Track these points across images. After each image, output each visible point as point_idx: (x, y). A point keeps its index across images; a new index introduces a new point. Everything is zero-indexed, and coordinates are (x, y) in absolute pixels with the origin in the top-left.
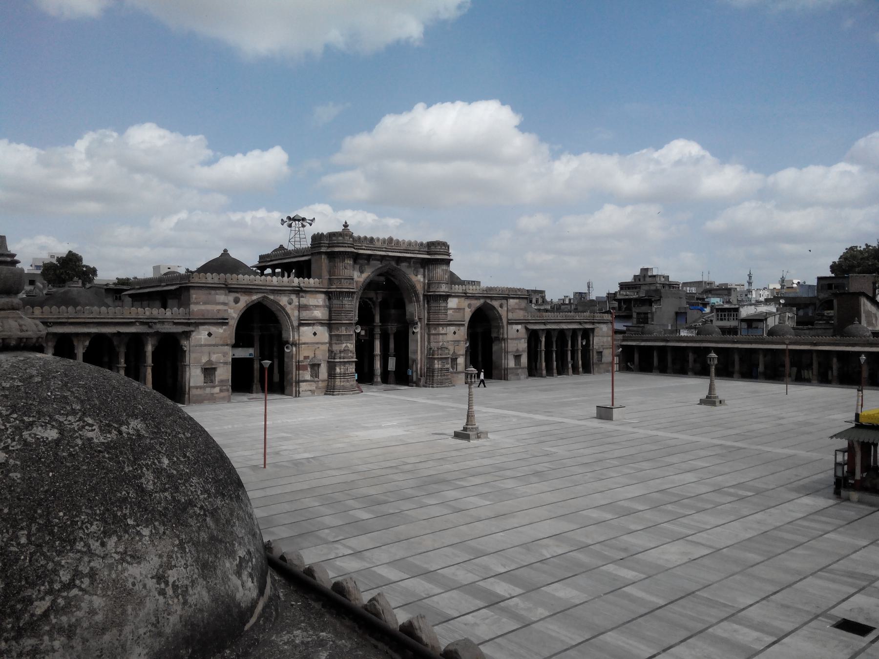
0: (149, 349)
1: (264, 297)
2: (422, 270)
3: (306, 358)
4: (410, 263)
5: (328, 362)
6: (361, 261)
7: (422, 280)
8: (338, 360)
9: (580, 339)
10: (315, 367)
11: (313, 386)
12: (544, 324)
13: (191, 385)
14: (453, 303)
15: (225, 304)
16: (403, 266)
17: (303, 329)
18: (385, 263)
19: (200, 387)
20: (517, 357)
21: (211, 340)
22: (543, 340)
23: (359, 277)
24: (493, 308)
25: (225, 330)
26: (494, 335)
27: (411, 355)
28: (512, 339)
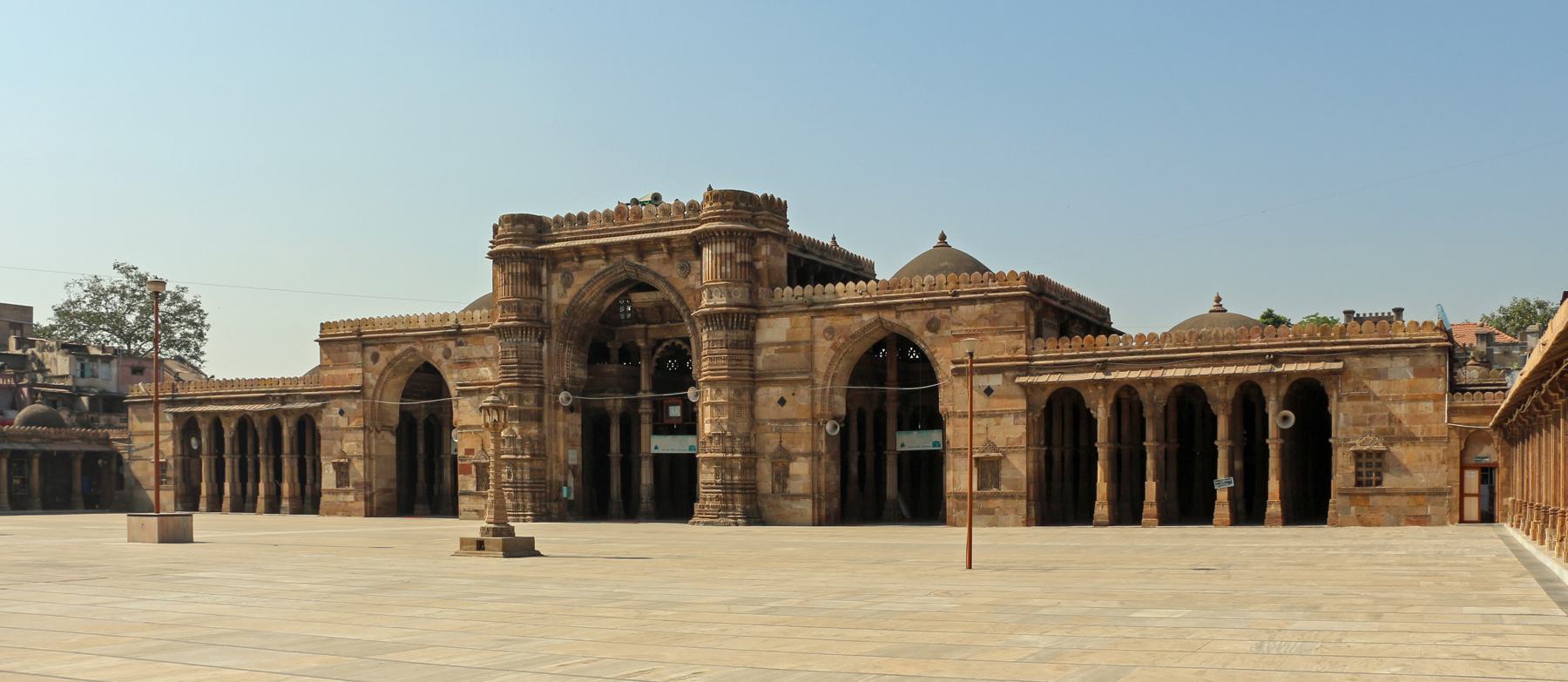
1: (413, 350)
3: (469, 451)
6: (564, 265)
9: (1271, 407)
12: (1104, 367)
14: (773, 331)
16: (655, 261)
22: (1102, 414)
23: (561, 296)
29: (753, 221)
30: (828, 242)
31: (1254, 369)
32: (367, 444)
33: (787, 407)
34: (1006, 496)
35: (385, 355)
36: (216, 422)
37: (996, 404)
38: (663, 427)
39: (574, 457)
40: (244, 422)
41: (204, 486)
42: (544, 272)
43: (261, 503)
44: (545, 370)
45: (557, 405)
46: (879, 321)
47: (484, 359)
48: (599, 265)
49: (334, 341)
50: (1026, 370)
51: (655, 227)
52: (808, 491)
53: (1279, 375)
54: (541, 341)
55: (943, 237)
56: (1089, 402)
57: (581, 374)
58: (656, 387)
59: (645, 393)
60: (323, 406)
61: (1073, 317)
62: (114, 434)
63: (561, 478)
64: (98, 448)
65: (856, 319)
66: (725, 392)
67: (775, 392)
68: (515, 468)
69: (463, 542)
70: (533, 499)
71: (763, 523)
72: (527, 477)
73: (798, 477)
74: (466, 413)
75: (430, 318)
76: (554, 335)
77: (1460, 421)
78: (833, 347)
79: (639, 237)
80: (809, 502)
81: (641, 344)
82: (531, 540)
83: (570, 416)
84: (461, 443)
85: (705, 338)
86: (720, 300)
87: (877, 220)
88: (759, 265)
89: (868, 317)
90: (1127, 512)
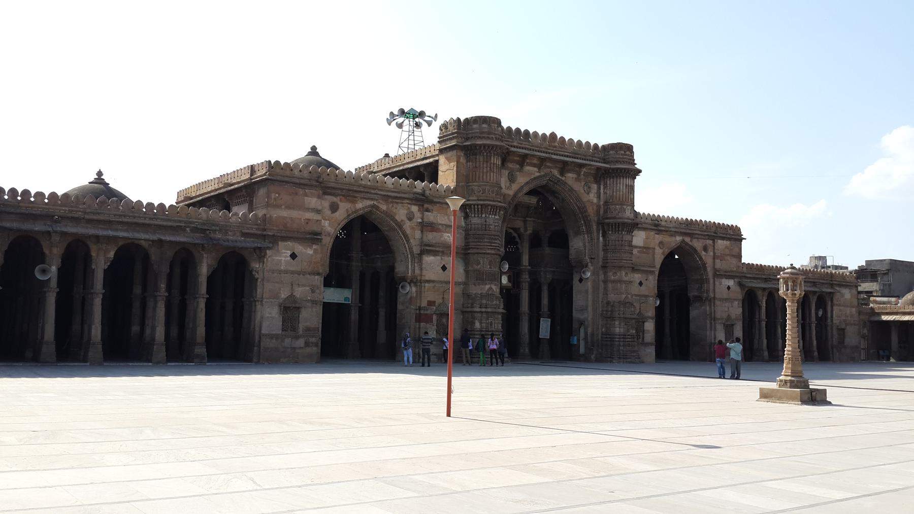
0: (204, 270)
1: (373, 206)
2: (595, 186)
3: (431, 303)
4: (579, 174)
5: (463, 312)
6: (510, 165)
7: (595, 200)
8: (478, 310)
13: (263, 332)
14: (639, 238)
15: (318, 212)
16: (570, 177)
17: (428, 259)
19: (276, 337)
21: (295, 266)
23: (508, 188)
24: (695, 250)
25: (316, 251)
26: (692, 293)
27: (576, 315)
33: (643, 287)
46: (683, 241)
52: (653, 341)
60: (269, 248)
65: (673, 239)
67: (637, 277)
77: (862, 317)
78: (663, 253)
80: (654, 347)
89: (679, 238)
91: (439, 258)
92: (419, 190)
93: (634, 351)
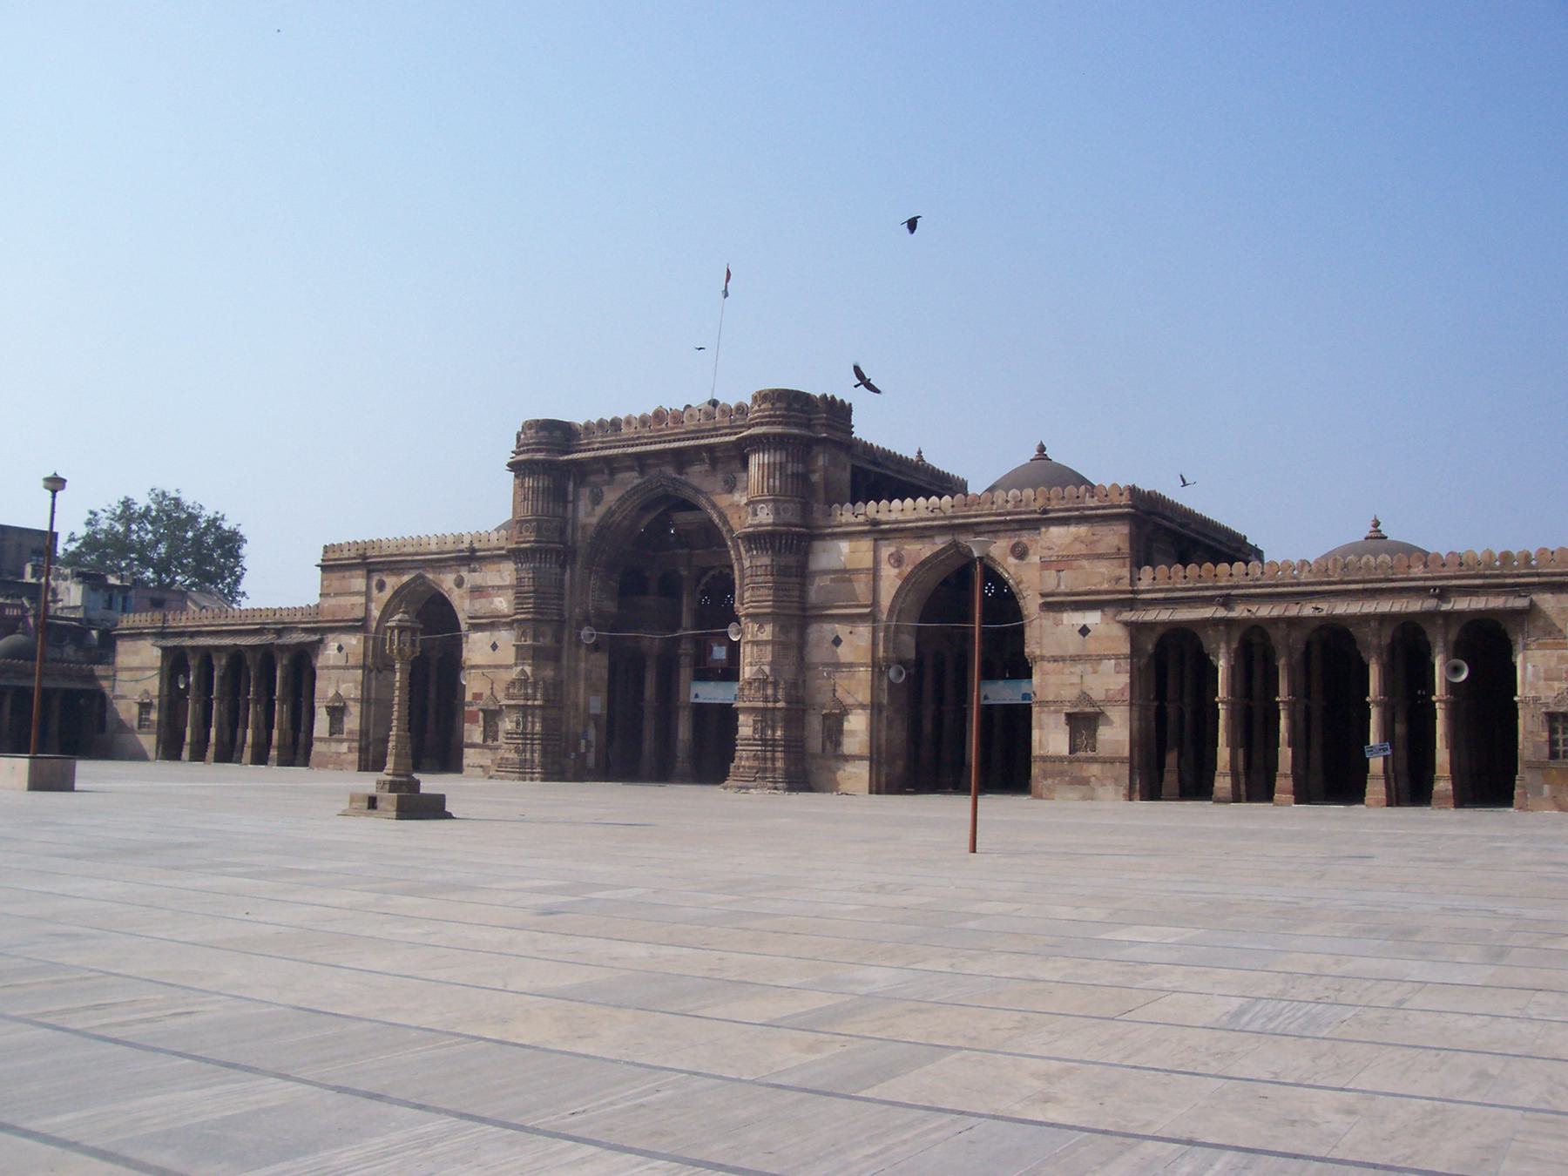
3: (477, 696)
6: (593, 479)
10: (491, 717)
11: (486, 758)
12: (1227, 601)
16: (696, 475)
18: (654, 472)
20: (1083, 723)
28: (1055, 660)
29: (809, 426)
30: (912, 455)
31: (1415, 606)
32: (366, 686)
34: (1104, 761)
35: (393, 582)
36: (207, 655)
37: (1092, 646)
38: (705, 672)
39: (597, 705)
40: (236, 655)
41: (188, 731)
42: (571, 485)
43: (248, 752)
44: (566, 602)
45: (579, 643)
47: (500, 588)
48: (632, 479)
49: (334, 564)
50: (1131, 604)
51: (697, 433)
52: (866, 751)
53: (1448, 614)
54: (563, 567)
55: (1042, 449)
56: (1208, 646)
57: (610, 606)
58: (701, 619)
59: (687, 630)
60: (321, 641)
61: (1194, 543)
62: (99, 670)
63: (580, 729)
64: (80, 686)
66: (768, 628)
68: (525, 717)
69: (353, 799)
70: (544, 753)
71: (810, 789)
72: (538, 727)
73: (853, 733)
74: (477, 649)
75: (442, 540)
76: (579, 559)
79: (676, 445)
80: (866, 764)
81: (684, 573)
82: (441, 799)
83: (597, 655)
84: (472, 684)
85: (747, 564)
86: (765, 516)
87: (950, 416)
88: (816, 477)
90: (1256, 785)
91: (487, 633)
92: (466, 545)
93: (765, 770)
